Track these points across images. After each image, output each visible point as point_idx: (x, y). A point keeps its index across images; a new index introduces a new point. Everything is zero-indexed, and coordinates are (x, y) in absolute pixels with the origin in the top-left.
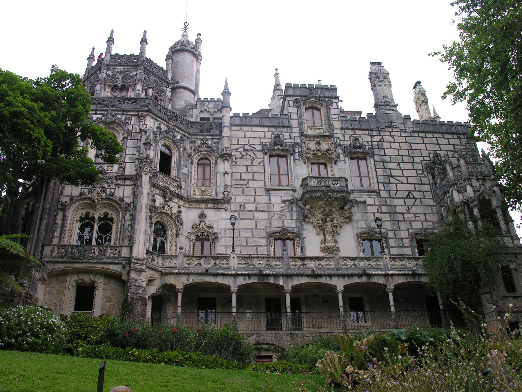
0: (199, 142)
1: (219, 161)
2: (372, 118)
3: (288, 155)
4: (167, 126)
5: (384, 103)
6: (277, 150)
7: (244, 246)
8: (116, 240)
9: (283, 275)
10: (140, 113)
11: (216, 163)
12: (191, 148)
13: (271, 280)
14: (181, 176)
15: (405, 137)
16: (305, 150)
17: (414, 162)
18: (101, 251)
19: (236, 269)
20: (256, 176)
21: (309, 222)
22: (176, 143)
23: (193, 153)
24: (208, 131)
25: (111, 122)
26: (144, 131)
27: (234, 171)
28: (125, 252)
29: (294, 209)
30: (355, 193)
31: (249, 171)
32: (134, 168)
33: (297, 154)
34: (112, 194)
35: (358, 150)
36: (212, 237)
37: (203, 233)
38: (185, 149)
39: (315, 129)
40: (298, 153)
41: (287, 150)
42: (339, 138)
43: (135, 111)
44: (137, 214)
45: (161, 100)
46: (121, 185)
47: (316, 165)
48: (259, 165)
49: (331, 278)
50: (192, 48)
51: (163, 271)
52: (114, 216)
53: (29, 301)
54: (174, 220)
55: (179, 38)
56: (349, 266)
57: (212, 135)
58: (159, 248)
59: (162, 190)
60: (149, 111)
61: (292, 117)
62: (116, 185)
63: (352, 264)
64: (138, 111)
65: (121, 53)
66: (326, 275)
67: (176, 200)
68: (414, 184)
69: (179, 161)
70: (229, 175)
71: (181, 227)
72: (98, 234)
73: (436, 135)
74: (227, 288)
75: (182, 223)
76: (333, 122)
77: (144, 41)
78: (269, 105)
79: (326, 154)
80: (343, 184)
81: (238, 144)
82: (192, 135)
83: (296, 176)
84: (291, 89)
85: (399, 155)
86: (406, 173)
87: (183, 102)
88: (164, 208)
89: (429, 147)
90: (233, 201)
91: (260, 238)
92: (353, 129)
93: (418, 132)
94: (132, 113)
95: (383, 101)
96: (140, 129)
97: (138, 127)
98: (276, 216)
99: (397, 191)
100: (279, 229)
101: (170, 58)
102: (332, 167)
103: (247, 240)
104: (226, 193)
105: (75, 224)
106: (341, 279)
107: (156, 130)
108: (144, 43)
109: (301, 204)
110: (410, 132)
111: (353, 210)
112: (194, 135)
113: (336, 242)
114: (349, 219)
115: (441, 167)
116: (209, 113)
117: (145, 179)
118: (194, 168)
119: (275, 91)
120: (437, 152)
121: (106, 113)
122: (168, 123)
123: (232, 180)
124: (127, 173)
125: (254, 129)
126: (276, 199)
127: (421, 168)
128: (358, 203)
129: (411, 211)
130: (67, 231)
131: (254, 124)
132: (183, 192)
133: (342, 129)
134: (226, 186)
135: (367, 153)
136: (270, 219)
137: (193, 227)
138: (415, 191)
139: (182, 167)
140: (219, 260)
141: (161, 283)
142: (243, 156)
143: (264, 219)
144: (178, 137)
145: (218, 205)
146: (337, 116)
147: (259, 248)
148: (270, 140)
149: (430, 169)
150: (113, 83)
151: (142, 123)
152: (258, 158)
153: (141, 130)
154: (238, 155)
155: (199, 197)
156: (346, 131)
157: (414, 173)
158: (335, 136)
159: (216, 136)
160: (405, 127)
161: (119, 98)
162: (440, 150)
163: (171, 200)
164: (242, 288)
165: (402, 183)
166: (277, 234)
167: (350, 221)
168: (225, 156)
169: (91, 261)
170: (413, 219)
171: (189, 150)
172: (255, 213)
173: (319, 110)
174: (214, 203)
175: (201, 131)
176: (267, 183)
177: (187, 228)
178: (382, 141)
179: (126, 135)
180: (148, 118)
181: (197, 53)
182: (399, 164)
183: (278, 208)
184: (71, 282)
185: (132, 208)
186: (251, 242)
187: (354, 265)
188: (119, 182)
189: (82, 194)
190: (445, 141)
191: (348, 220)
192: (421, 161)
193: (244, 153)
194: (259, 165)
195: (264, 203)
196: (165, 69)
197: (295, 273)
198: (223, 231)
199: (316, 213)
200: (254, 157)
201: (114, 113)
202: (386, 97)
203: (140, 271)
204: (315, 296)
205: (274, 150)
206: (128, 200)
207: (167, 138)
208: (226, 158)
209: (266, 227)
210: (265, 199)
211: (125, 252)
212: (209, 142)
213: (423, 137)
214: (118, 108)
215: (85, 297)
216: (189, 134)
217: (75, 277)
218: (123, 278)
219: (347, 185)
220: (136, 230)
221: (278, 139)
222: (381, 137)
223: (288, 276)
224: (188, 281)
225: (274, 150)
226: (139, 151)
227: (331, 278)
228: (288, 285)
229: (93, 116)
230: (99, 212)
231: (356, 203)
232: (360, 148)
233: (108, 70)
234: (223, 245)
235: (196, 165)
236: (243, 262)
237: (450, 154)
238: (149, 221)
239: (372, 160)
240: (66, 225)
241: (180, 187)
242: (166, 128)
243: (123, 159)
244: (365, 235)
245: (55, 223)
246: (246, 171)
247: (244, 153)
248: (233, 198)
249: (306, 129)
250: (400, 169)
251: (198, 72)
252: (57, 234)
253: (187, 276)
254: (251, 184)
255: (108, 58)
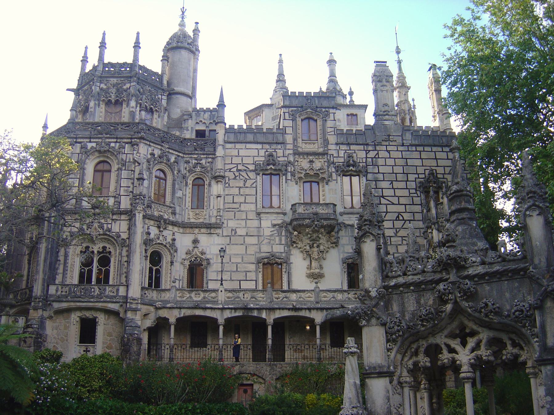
0: (194, 161)
1: (213, 182)
2: (370, 131)
3: (281, 175)
4: (161, 149)
5: (384, 112)
6: (272, 169)
7: (234, 272)
8: (114, 275)
9: (266, 309)
10: (133, 140)
11: (210, 185)
12: (186, 169)
13: (255, 313)
14: (176, 201)
15: (402, 151)
16: (298, 169)
17: (408, 181)
18: (100, 289)
19: (223, 302)
20: (249, 199)
21: (297, 247)
22: (170, 166)
23: (188, 174)
24: (203, 149)
25: (105, 151)
26: (138, 163)
27: (226, 193)
28: (122, 291)
29: (283, 234)
30: (344, 216)
31: (241, 193)
32: (129, 202)
33: (289, 174)
34: (109, 230)
35: (351, 168)
36: (204, 263)
37: (196, 258)
38: (179, 171)
39: (310, 143)
40: (291, 172)
41: (280, 170)
42: (333, 155)
43: (128, 138)
44: (132, 255)
45: (156, 111)
46: (117, 220)
47: (309, 184)
48: (251, 187)
49: (310, 312)
50: (188, 44)
51: (157, 306)
52: (112, 250)
53: (40, 340)
54: (168, 249)
55: (175, 29)
56: (328, 299)
57: (206, 154)
58: (154, 281)
59: (156, 221)
60: (142, 138)
61: (287, 132)
62: (112, 220)
63: (332, 296)
64: (131, 138)
65: (114, 61)
66: (305, 309)
67: (170, 227)
68: (405, 205)
69: (174, 185)
70: (222, 198)
71: (175, 254)
72: (98, 267)
73: (434, 149)
74: (214, 321)
75: (176, 251)
76: (329, 136)
77: (137, 46)
78: (271, 99)
79: (318, 174)
80: (331, 211)
81: (232, 163)
82: (186, 154)
83: (287, 198)
84: (288, 98)
85: (393, 173)
86: (398, 193)
87: (179, 111)
88: (158, 238)
89: (426, 162)
90: (225, 225)
91: (250, 263)
92: (348, 144)
93: (416, 146)
94: (125, 140)
95: (383, 110)
96: (134, 159)
97: (131, 156)
98: (266, 241)
99: (387, 212)
100: (268, 254)
101: (165, 60)
102: (323, 187)
103: (237, 265)
104: (218, 217)
105: (76, 258)
106: (319, 312)
107: (149, 156)
108: (137, 48)
109: (290, 228)
110: (408, 146)
111: (342, 233)
112: (188, 154)
113: (321, 267)
114: (336, 244)
115: (435, 185)
116: (204, 125)
117: (139, 217)
118: (189, 191)
119: (277, 81)
120: (433, 168)
121: (100, 140)
122: (162, 146)
123: (224, 203)
124: (123, 206)
125: (248, 146)
126: (267, 223)
127: (415, 187)
128: (346, 226)
129: (398, 235)
130: (69, 267)
131: (248, 140)
132: (178, 218)
133: (337, 144)
134: (219, 210)
135: (360, 171)
136: (259, 244)
137: (187, 254)
138: (406, 212)
139: (176, 191)
140: (208, 293)
141: (156, 316)
142: (236, 177)
143: (254, 245)
144: (173, 159)
145: (210, 230)
146: (333, 129)
147: (248, 274)
148: (263, 159)
149: (424, 188)
150: (107, 98)
151: (135, 152)
152: (251, 179)
153: (135, 161)
154: (231, 175)
155: (192, 220)
156: (341, 146)
157: (406, 193)
158: (330, 152)
159: (210, 154)
160: (403, 140)
161: (112, 123)
162: (437, 166)
163: (165, 229)
164: (228, 321)
165: (393, 204)
166: (266, 260)
167: (336, 246)
168: (218, 178)
169: (92, 300)
170: (400, 243)
171: (183, 172)
172: (246, 237)
173: (316, 121)
174: (207, 228)
175: (196, 149)
176: (258, 207)
177: (181, 254)
178: (377, 156)
179: (120, 166)
180: (141, 145)
181: (194, 49)
182: (392, 183)
183: (267, 232)
184: (75, 317)
185: (127, 244)
186: (241, 267)
187: (334, 297)
188: (115, 217)
189: (81, 229)
190: (444, 155)
191: (334, 245)
192: (416, 178)
193: (237, 174)
194: (251, 187)
195: (254, 228)
196: (160, 73)
197: (276, 306)
198: (215, 257)
199: (304, 238)
200: (247, 177)
201: (107, 140)
202: (386, 105)
203: (135, 310)
204: (298, 321)
205: (267, 170)
206: (124, 236)
207: (161, 162)
208: (219, 180)
209: (256, 252)
210: (256, 223)
211: (122, 291)
212: (203, 162)
213: (420, 151)
214: (111, 135)
215: (88, 333)
216: (184, 154)
217: (79, 314)
218: (121, 316)
219: (335, 212)
220: (131, 271)
221: (271, 158)
222: (376, 152)
223: (271, 309)
224: (180, 314)
225: (267, 170)
226: (133, 183)
227: (310, 312)
228: (270, 319)
229: (88, 144)
230: (98, 246)
231: (345, 226)
232: (353, 166)
233: (101, 83)
234: (215, 271)
235: (191, 186)
236: (230, 295)
237: (448, 170)
238: (144, 254)
239: (364, 178)
240: (68, 261)
241: (174, 213)
242: (160, 152)
243: (118, 193)
244: (350, 260)
245: (58, 260)
246: (238, 193)
247: (237, 174)
248: (225, 222)
249: (300, 145)
250: (393, 188)
251: (195, 71)
252: (61, 270)
253: (179, 310)
254: (243, 207)
255: (100, 68)
